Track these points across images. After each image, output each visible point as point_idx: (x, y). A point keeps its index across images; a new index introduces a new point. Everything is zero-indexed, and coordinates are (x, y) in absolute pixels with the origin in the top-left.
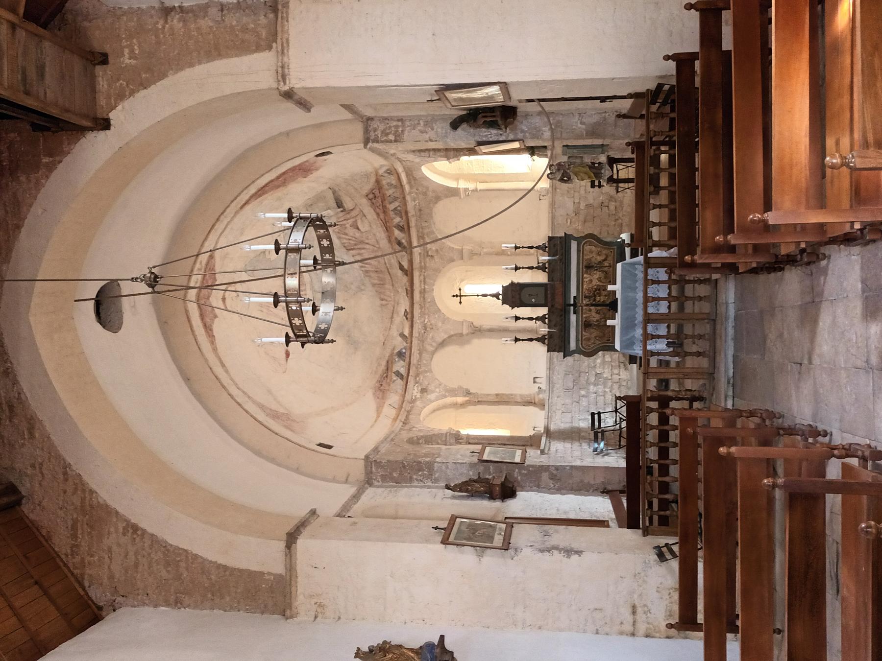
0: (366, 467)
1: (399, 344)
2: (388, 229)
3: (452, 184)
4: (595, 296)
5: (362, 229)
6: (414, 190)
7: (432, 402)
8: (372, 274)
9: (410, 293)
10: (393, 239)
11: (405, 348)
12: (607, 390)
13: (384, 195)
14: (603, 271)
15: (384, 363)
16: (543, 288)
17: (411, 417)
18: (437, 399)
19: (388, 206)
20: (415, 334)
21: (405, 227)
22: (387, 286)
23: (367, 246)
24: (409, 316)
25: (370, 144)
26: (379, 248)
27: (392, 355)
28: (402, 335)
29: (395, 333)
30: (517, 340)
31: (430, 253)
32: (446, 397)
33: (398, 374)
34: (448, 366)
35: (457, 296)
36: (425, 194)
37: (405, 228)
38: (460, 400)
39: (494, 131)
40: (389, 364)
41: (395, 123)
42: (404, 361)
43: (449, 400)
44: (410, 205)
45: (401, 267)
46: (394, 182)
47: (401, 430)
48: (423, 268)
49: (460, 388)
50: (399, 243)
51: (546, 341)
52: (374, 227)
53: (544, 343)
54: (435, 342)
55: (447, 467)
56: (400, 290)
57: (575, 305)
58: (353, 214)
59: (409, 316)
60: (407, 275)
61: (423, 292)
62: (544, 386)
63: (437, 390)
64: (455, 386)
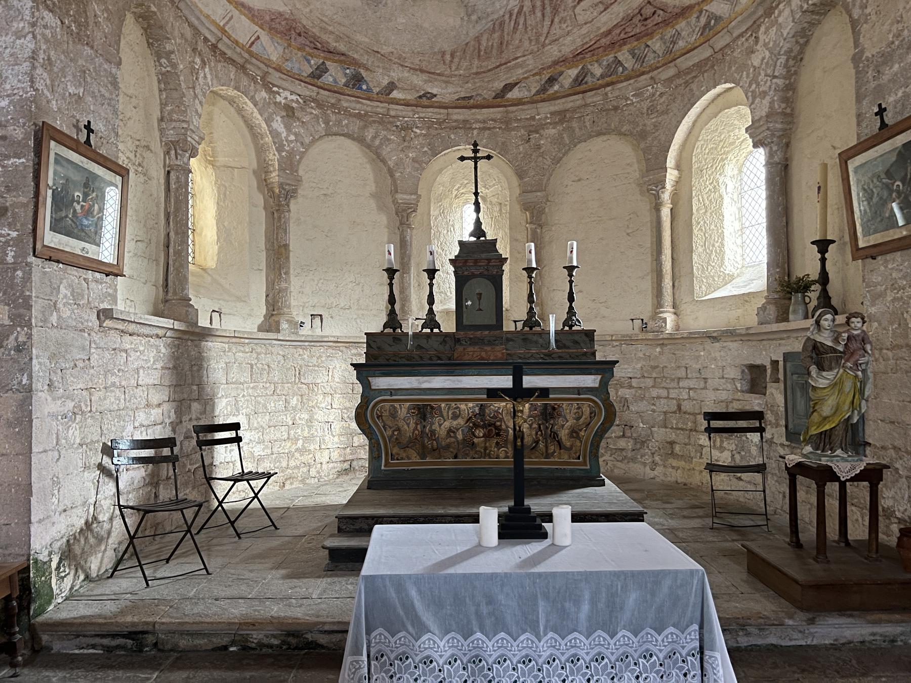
1: (378, 79)
2: (578, 56)
3: (671, 162)
4: (483, 427)
6: (660, 88)
7: (268, 121)
9: (466, 103)
10: (559, 68)
11: (369, 90)
13: (650, 34)
15: (342, 47)
17: (233, 70)
19: (626, 48)
20: (395, 110)
21: (583, 87)
23: (547, 23)
24: (426, 99)
26: (544, 46)
27: (355, 63)
28: (392, 86)
29: (396, 74)
30: (391, 272)
32: (280, 149)
33: (321, 71)
34: (338, 168)
36: (651, 110)
38: (274, 177)
43: (273, 157)
44: (627, 89)
45: (509, 87)
46: (681, 44)
47: (197, 32)
49: (299, 180)
50: (552, 80)
51: (388, 330)
52: (584, 30)
53: (385, 327)
54: (381, 144)
55: (19, 35)
57: (518, 393)
60: (495, 98)
61: (466, 125)
62: (305, 331)
63: (292, 138)
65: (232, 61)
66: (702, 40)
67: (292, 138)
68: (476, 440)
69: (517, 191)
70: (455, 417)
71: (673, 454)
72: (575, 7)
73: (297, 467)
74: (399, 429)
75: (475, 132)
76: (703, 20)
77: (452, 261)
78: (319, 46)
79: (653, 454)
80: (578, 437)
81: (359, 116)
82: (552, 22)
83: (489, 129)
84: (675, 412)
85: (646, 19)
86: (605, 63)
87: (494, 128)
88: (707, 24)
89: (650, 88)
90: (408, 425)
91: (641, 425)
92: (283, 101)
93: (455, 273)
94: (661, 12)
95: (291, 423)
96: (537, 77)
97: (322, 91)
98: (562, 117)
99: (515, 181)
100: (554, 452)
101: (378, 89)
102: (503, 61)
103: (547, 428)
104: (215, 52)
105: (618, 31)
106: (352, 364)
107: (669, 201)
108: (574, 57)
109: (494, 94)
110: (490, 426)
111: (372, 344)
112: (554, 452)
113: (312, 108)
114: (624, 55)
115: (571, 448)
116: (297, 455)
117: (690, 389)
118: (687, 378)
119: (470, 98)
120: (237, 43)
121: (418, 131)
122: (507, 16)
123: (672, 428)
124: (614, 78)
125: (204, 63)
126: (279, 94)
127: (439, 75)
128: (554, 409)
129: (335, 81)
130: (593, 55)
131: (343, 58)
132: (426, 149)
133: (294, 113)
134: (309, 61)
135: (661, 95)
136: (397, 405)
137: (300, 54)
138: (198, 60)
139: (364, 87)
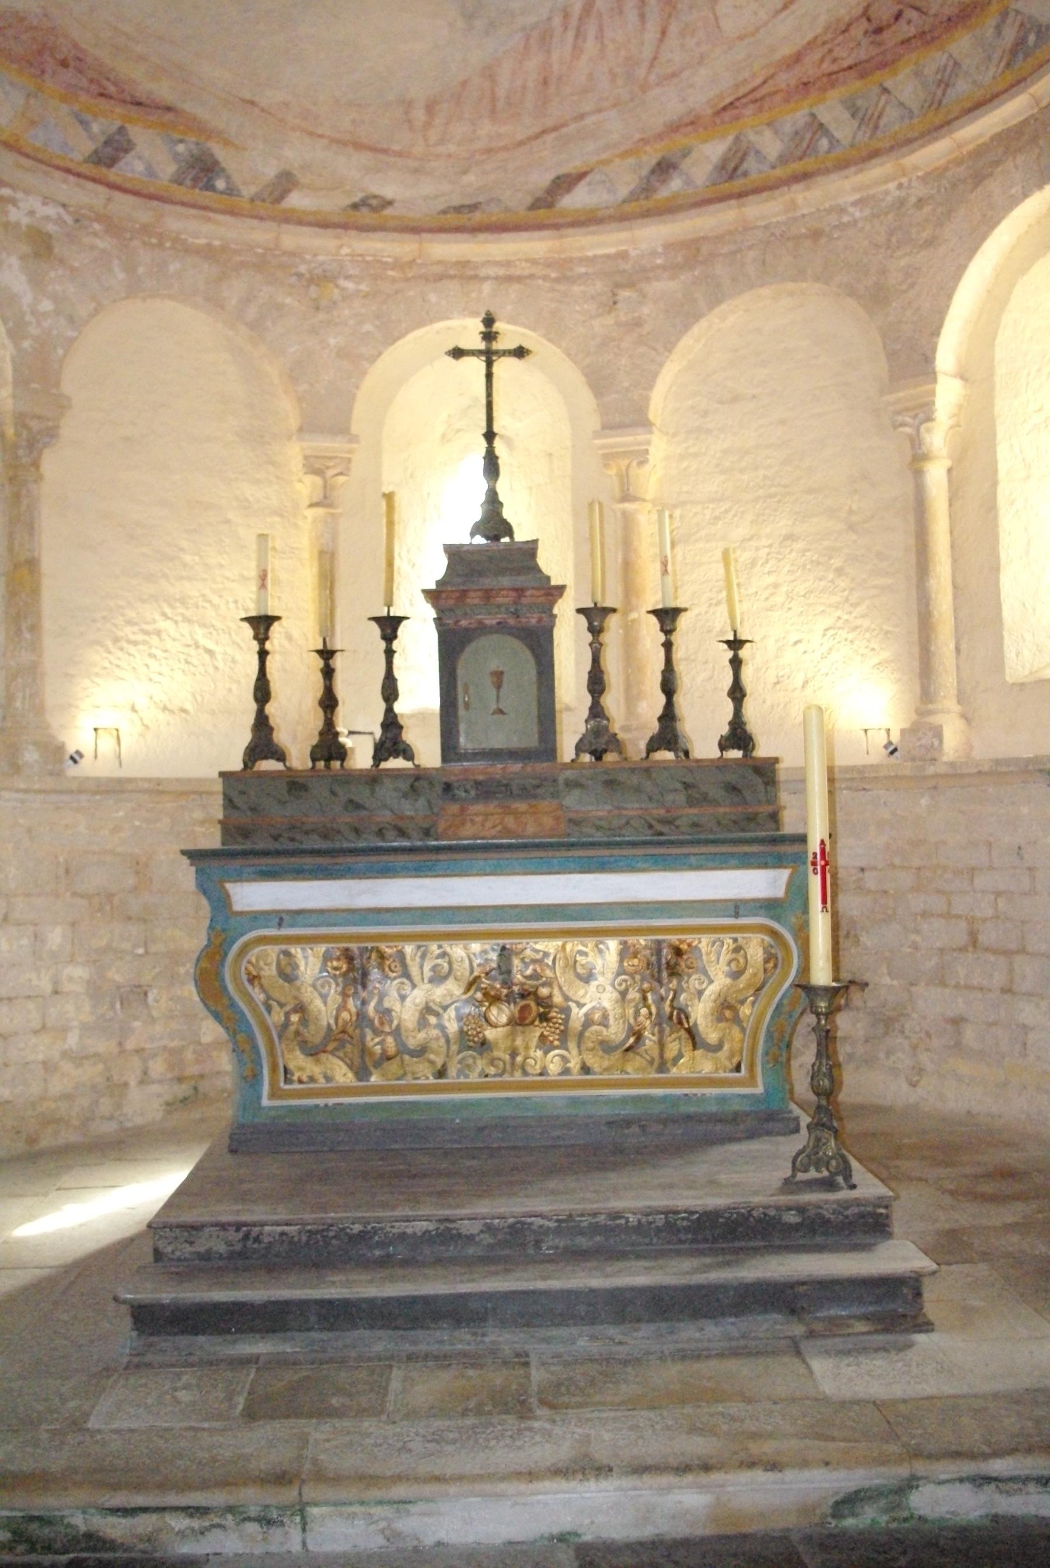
1: (250, 166)
2: (728, 110)
4: (509, 999)
8: (533, 63)
10: (680, 140)
11: (231, 191)
12: (73, 1040)
15: (164, 91)
16: (532, 741)
19: (834, 96)
20: (293, 238)
21: (738, 184)
22: (486, 128)
23: (651, 34)
26: (645, 88)
28: (286, 183)
29: (295, 153)
31: (624, 294)
37: (733, 181)
42: (178, 180)
44: (841, 189)
45: (565, 183)
46: (962, 87)
48: (563, 271)
49: (62, 405)
50: (664, 168)
56: (470, 178)
59: (367, 214)
60: (534, 207)
61: (465, 273)
63: (46, 305)
64: (67, 387)
66: (1010, 78)
67: (46, 305)
69: (593, 422)
70: (438, 978)
71: (958, 1047)
73: (68, 1097)
74: (301, 1008)
75: (487, 287)
76: (1010, 34)
77: (431, 596)
78: (112, 89)
79: (915, 1048)
80: (736, 1020)
81: (208, 253)
82: (664, 33)
83: (519, 279)
84: (962, 950)
85: (879, 30)
86: (788, 128)
87: (532, 276)
88: (1020, 43)
89: (892, 186)
90: (324, 998)
91: (887, 980)
92: (25, 221)
93: (439, 622)
95: (48, 988)
96: (631, 160)
97: (117, 195)
98: (691, 254)
99: (586, 399)
100: (680, 1056)
101: (253, 190)
102: (550, 122)
103: (663, 999)
105: (817, 55)
106: (184, 853)
107: (944, 452)
108: (718, 113)
109: (529, 200)
110: (523, 996)
111: (238, 801)
113: (95, 234)
114: (831, 111)
115: (719, 1047)
116: (67, 1066)
117: (998, 894)
118: (991, 868)
119: (474, 207)
121: (350, 285)
122: (557, 21)
123: (957, 986)
124: (808, 164)
126: (14, 202)
127: (400, 154)
128: (678, 952)
129: (150, 172)
130: (760, 110)
131: (169, 117)
132: (368, 327)
133: (49, 248)
134: (84, 123)
135: (920, 202)
136: (296, 951)
137: (64, 108)
139: (220, 184)
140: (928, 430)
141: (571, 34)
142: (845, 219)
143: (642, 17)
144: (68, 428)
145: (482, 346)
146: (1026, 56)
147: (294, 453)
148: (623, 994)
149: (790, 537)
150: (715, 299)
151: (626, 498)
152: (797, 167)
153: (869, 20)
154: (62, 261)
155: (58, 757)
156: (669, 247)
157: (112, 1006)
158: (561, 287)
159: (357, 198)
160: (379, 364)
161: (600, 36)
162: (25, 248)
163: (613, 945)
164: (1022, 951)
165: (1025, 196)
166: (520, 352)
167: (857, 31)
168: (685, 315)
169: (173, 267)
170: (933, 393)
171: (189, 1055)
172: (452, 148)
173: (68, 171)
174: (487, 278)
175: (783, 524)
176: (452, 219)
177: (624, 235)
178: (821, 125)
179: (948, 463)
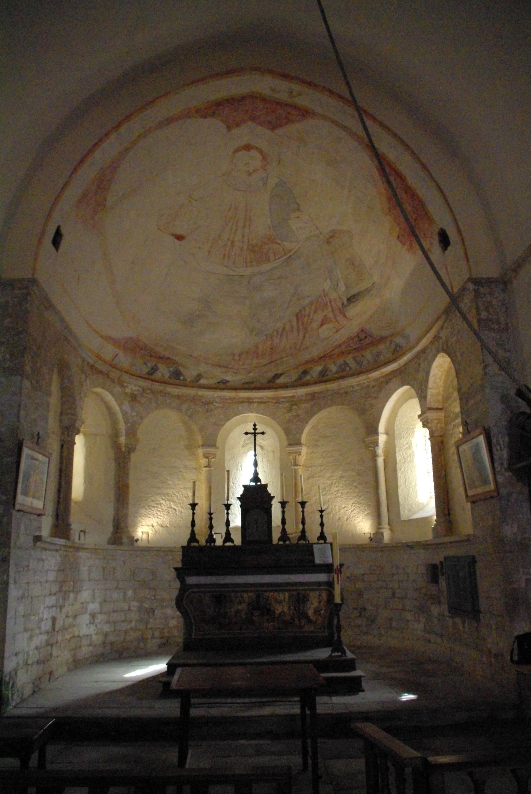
0: (21, 280)
1: (190, 373)
2: (322, 358)
3: (382, 428)
5: (320, 330)
7: (120, 405)
8: (269, 343)
10: (310, 365)
11: (185, 380)
12: (133, 624)
14: (293, 619)
15: (167, 354)
18: (124, 414)
19: (350, 356)
20: (201, 392)
21: (325, 378)
22: (255, 361)
23: (301, 337)
25: (471, 286)
29: (202, 368)
31: (294, 407)
32: (126, 423)
33: (154, 369)
35: (255, 429)
37: (324, 378)
38: (123, 440)
39: (505, 454)
40: (167, 360)
41: (502, 319)
43: (122, 427)
44: (353, 381)
45: (277, 376)
46: (382, 358)
47: (84, 360)
50: (305, 373)
56: (251, 374)
58: (340, 317)
59: (223, 385)
61: (250, 401)
63: (135, 414)
64: (139, 435)
65: (101, 372)
67: (135, 414)
68: (254, 618)
69: (285, 443)
70: (240, 603)
72: (318, 329)
75: (255, 405)
76: (393, 346)
80: (320, 615)
82: (304, 336)
83: (264, 403)
85: (361, 340)
86: (338, 364)
87: (268, 402)
88: (395, 350)
92: (130, 391)
93: (241, 506)
94: (370, 338)
95: (127, 609)
97: (154, 383)
98: (313, 396)
100: (305, 624)
102: (273, 360)
104: (92, 369)
106: (174, 568)
107: (382, 454)
112: (305, 624)
113: (148, 394)
114: (349, 360)
120: (105, 362)
121: (217, 405)
122: (275, 333)
124: (344, 373)
125: (87, 377)
126: (127, 386)
128: (304, 597)
129: (163, 375)
131: (168, 361)
133: (135, 398)
134: (146, 364)
135: (373, 386)
138: (83, 376)
139: (182, 378)
140: (378, 449)
141: (279, 337)
142: (354, 389)
143: (298, 332)
144: (138, 447)
145: (253, 431)
146: (397, 352)
147: (200, 452)
148: (289, 607)
149: (341, 477)
150: (320, 409)
151: (296, 465)
152: (342, 374)
153: (359, 337)
154: (139, 402)
155: (133, 541)
156: (307, 395)
157: (145, 615)
158: (277, 405)
159: (219, 380)
160: (225, 426)
161: (287, 337)
162: (130, 399)
163: (287, 594)
164: (406, 597)
165: (399, 388)
166: (263, 433)
167: (356, 339)
168: (311, 414)
169: (168, 401)
170: (378, 439)
171: (166, 630)
172: (246, 367)
173: (141, 377)
174: (256, 402)
175: (339, 473)
176: (247, 386)
177: (294, 391)
178: (347, 364)
179: (383, 457)
